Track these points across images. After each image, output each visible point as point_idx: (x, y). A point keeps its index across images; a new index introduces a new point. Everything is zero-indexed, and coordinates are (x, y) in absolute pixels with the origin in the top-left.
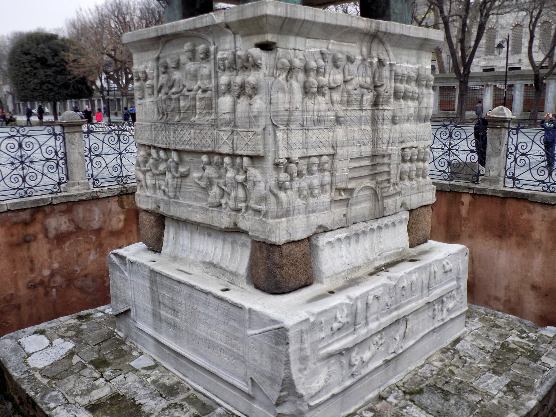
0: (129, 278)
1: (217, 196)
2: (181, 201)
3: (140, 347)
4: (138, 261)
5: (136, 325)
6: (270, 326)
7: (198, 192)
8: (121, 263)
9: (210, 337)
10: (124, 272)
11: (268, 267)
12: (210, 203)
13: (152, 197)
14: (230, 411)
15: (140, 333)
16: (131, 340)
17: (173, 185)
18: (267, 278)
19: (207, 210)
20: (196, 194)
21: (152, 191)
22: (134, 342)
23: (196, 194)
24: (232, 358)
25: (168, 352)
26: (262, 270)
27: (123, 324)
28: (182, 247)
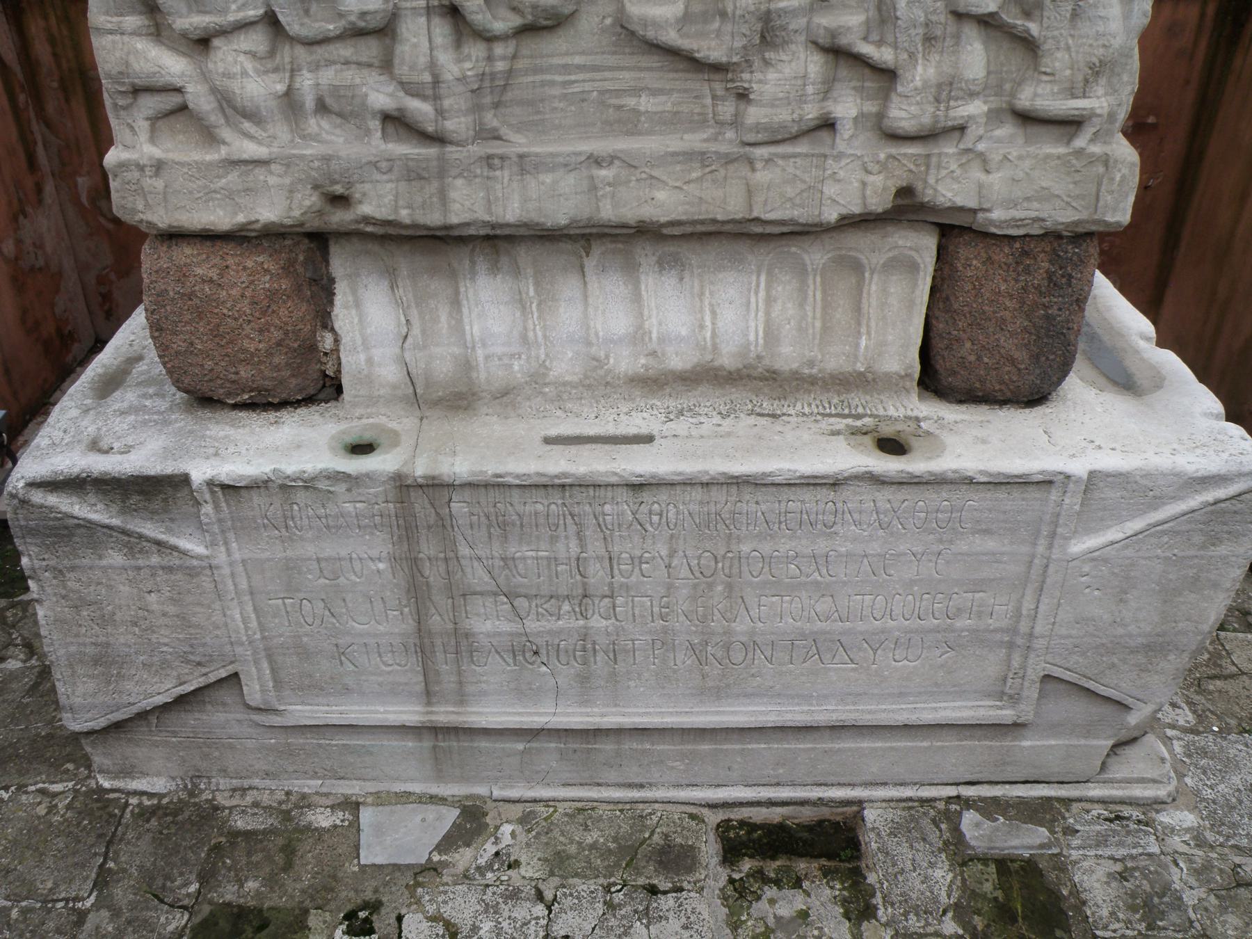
0: (221, 557)
1: (810, 89)
2: (520, 143)
3: (310, 786)
4: (291, 467)
5: (276, 720)
6: (1181, 499)
7: (636, 91)
8: (124, 511)
9: (819, 625)
10: (173, 540)
11: (1048, 318)
12: (757, 128)
13: (288, 163)
14: (910, 799)
15: (297, 740)
16: (224, 783)
17: (462, 79)
18: (1035, 358)
19: (729, 160)
20: (631, 102)
21: (281, 131)
22: (256, 782)
23: (631, 102)
24: (938, 652)
25: (520, 746)
26: (1012, 334)
27: (156, 745)
28: (484, 345)
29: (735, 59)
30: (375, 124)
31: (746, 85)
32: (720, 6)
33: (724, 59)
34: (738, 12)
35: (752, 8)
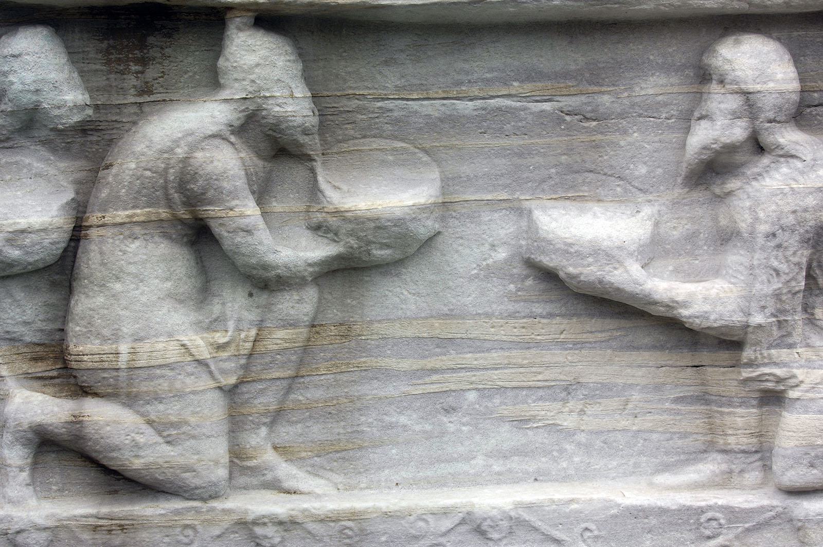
29: (758, 319)
30: (16, 456)
31: (779, 372)
32: (723, 222)
33: (738, 318)
34: (763, 228)
35: (790, 220)
